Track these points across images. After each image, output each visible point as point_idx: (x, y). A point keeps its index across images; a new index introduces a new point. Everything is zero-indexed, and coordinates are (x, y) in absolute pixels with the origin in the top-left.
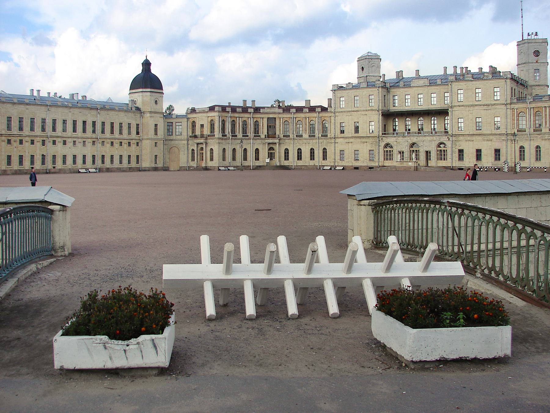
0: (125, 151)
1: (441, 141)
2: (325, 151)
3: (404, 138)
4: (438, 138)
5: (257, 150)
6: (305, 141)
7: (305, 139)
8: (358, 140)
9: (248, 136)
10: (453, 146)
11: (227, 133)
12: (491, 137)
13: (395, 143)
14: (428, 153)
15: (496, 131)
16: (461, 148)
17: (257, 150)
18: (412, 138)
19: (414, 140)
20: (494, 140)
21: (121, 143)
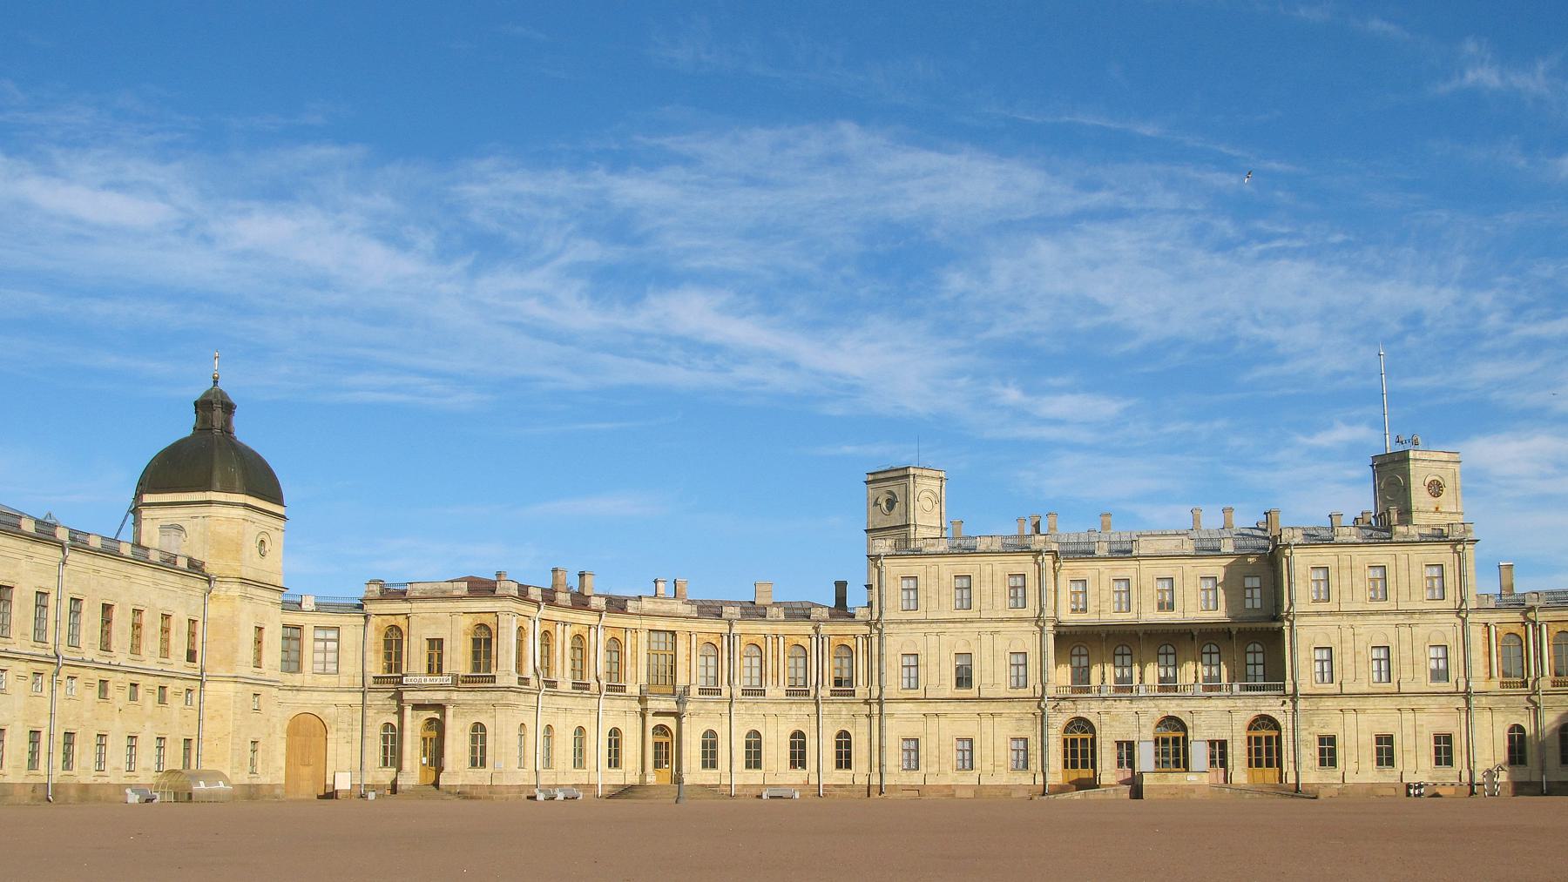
0: (147, 718)
1: (1263, 713)
2: (844, 744)
3: (1136, 706)
4: (1250, 705)
5: (615, 737)
6: (773, 709)
7: (775, 702)
8: (972, 708)
9: (586, 687)
10: (1302, 727)
11: (528, 672)
12: (1422, 701)
13: (1103, 717)
14: (1219, 751)
15: (1436, 684)
16: (1327, 732)
17: (615, 737)
18: (1163, 703)
19: (1172, 707)
20: (1434, 710)
21: (133, 688)
